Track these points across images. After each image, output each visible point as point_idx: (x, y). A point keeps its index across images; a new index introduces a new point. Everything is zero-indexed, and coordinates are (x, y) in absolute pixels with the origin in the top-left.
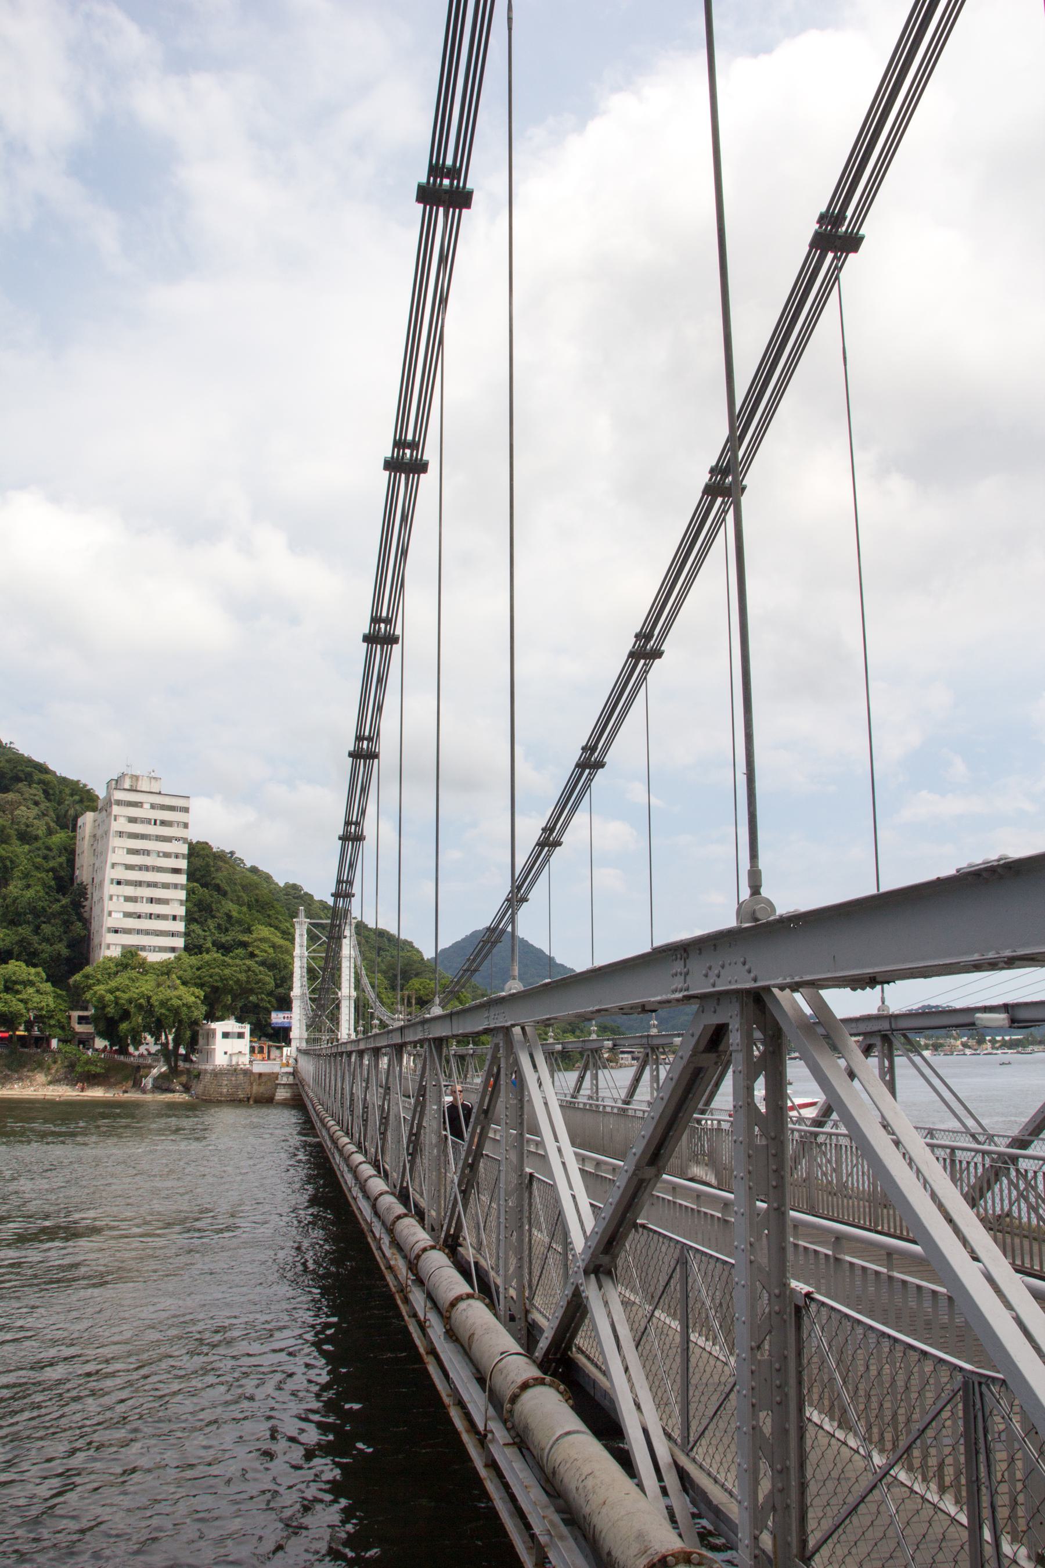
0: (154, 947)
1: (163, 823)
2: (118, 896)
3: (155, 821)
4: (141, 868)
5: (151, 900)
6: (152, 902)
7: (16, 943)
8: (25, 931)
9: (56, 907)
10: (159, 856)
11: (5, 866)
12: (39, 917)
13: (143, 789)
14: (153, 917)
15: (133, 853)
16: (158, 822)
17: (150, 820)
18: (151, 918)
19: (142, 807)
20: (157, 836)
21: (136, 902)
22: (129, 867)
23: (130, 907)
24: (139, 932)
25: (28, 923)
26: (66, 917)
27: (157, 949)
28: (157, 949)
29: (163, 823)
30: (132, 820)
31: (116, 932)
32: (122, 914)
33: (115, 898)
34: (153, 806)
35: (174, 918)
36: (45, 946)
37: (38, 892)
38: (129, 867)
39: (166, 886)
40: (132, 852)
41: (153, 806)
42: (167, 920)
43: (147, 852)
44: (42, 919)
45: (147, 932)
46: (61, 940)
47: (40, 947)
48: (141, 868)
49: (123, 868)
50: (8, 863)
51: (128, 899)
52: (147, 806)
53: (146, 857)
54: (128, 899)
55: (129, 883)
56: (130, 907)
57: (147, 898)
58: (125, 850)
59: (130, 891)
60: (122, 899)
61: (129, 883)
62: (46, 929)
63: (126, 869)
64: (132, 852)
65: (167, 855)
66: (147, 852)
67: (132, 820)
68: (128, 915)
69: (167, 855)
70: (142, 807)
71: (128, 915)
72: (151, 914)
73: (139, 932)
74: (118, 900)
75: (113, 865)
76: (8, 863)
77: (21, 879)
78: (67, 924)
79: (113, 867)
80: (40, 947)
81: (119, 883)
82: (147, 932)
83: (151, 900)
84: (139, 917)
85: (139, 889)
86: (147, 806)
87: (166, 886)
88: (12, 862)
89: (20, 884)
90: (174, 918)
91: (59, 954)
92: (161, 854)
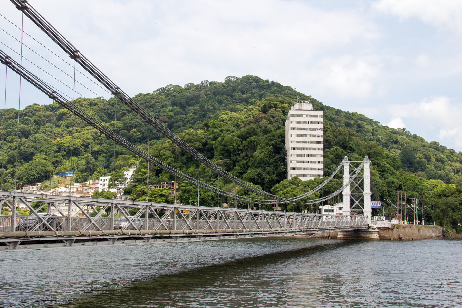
0: (311, 175)
1: (312, 123)
2: (294, 154)
3: (308, 122)
4: (303, 142)
5: (308, 155)
6: (308, 156)
7: (256, 175)
8: (259, 170)
9: (272, 160)
10: (311, 137)
11: (254, 145)
12: (265, 164)
13: (304, 109)
14: (309, 162)
15: (300, 136)
16: (310, 122)
17: (306, 122)
18: (308, 163)
19: (302, 117)
20: (309, 128)
21: (302, 156)
22: (298, 142)
23: (299, 159)
24: (304, 169)
25: (262, 167)
26: (276, 164)
27: (312, 176)
28: (312, 176)
29: (312, 123)
30: (298, 122)
31: (294, 169)
32: (296, 162)
33: (293, 155)
34: (307, 116)
35: (319, 162)
36: (267, 176)
37: (265, 154)
38: (298, 142)
39: (314, 149)
40: (299, 136)
41: (307, 116)
42: (316, 163)
43: (305, 135)
44: (267, 165)
45: (308, 169)
46: (274, 173)
47: (266, 176)
48: (303, 142)
49: (296, 142)
50: (255, 143)
51: (298, 155)
52: (304, 116)
53: (305, 137)
54: (298, 155)
55: (299, 149)
56: (299, 159)
57: (306, 155)
58: (296, 135)
59: (299, 152)
60: (296, 156)
61: (299, 149)
62: (268, 169)
63: (297, 143)
64: (299, 136)
65: (314, 136)
66: (305, 135)
67: (298, 122)
68: (298, 162)
69: (314, 136)
70: (302, 117)
71: (298, 162)
72: (308, 161)
73: (304, 169)
74: (294, 156)
75: (291, 142)
76: (255, 143)
77: (260, 149)
78: (277, 167)
79: (291, 143)
80: (266, 176)
81: (294, 149)
82: (308, 169)
83: (308, 155)
84: (303, 163)
85: (303, 151)
86: (304, 116)
87: (314, 149)
88: (257, 142)
89: (260, 151)
90: (319, 162)
91: (273, 180)
92: (312, 136)
